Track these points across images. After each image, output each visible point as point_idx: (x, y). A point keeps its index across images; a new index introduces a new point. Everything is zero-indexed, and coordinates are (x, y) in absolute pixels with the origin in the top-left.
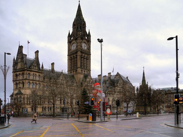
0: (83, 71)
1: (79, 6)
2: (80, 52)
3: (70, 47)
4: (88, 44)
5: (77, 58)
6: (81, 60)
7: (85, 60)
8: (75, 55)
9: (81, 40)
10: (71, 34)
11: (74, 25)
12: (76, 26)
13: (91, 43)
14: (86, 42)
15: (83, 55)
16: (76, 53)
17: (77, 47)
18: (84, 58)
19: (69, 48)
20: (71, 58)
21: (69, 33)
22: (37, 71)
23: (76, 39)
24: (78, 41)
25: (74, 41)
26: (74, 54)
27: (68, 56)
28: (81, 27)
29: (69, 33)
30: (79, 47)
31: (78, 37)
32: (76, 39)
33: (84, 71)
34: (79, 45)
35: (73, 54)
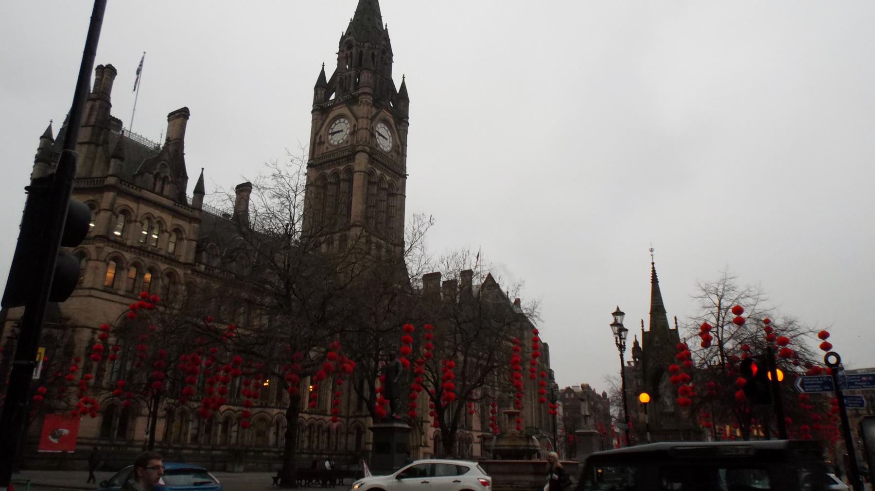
2: (366, 156)
4: (398, 132)
5: (350, 181)
6: (368, 196)
7: (383, 195)
8: (341, 168)
9: (374, 111)
10: (328, 77)
11: (346, 44)
12: (354, 50)
13: (410, 129)
14: (392, 121)
15: (378, 172)
16: (351, 157)
17: (353, 133)
18: (380, 189)
20: (323, 177)
21: (323, 74)
22: (169, 203)
23: (352, 101)
24: (362, 110)
25: (345, 110)
26: (339, 165)
27: (310, 166)
28: (373, 56)
29: (323, 74)
30: (363, 134)
31: (359, 95)
32: (352, 101)
33: (379, 247)
34: (365, 126)
35: (337, 161)
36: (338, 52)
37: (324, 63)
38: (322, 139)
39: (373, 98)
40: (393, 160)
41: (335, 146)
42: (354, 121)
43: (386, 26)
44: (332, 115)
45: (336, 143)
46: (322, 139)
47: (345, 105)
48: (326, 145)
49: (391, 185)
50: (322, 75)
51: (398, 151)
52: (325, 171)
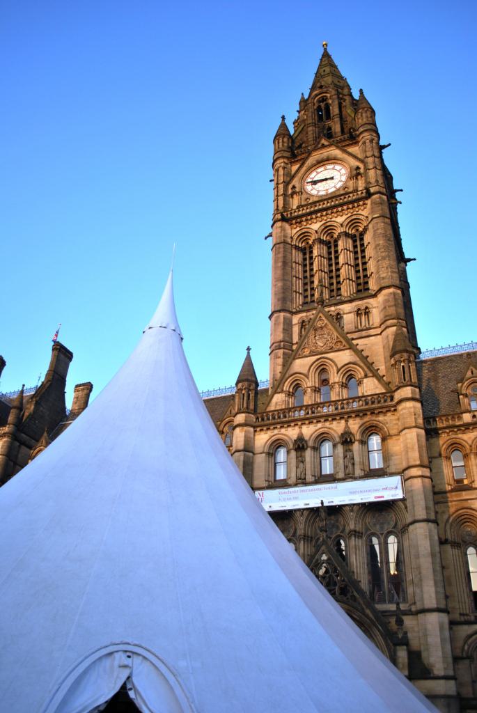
1: (326, 55)
8: (340, 220)
19: (286, 184)
29: (283, 126)
38: (297, 190)
46: (297, 190)
48: (304, 196)
50: (283, 126)
52: (311, 226)
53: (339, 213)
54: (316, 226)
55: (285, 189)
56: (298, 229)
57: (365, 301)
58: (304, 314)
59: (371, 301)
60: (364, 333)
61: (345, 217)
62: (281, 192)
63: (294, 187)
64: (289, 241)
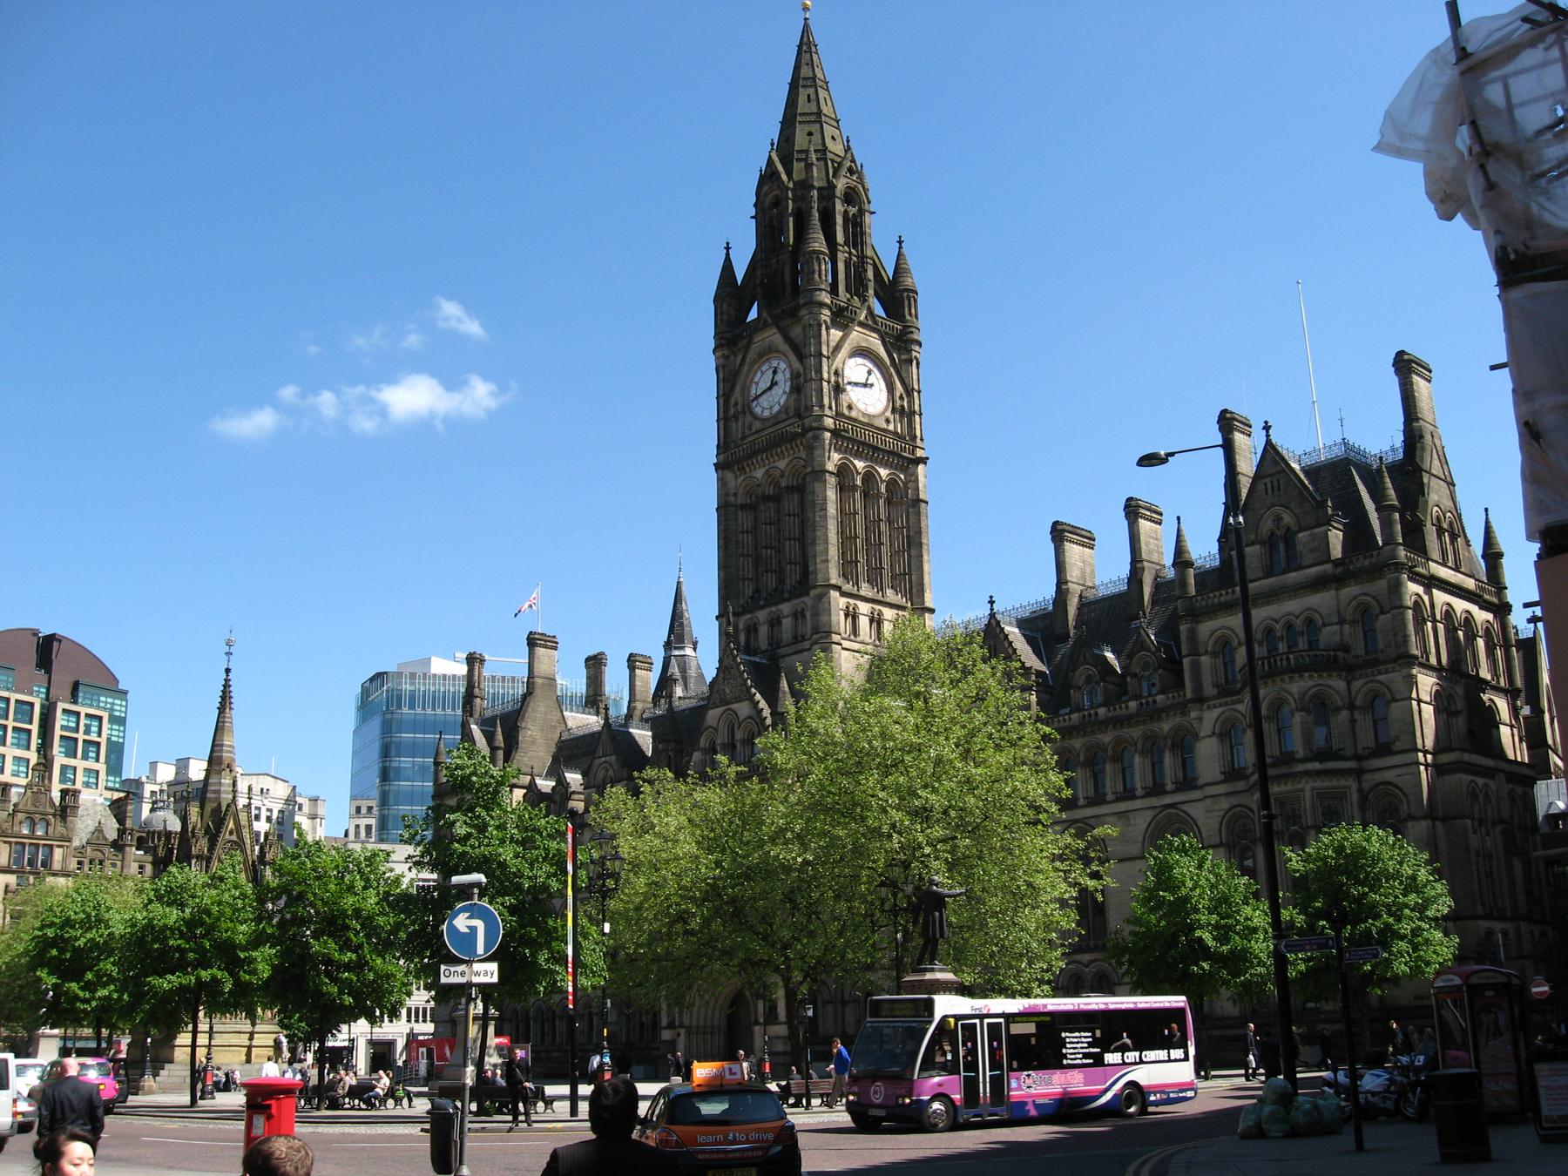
0: (864, 622)
3: (737, 395)
8: (782, 464)
9: (836, 334)
27: (718, 467)
29: (728, 267)
36: (754, 214)
37: (728, 243)
38: (739, 407)
39: (830, 309)
40: (891, 427)
41: (768, 419)
42: (797, 365)
43: (848, 141)
44: (751, 355)
45: (767, 413)
47: (775, 330)
48: (749, 418)
49: (892, 483)
50: (728, 267)
51: (902, 406)
53: (781, 456)
54: (759, 474)
55: (726, 411)
56: (743, 478)
57: (802, 599)
58: (749, 616)
59: (805, 599)
60: (799, 646)
61: (786, 461)
62: (721, 416)
63: (736, 404)
64: (732, 499)
